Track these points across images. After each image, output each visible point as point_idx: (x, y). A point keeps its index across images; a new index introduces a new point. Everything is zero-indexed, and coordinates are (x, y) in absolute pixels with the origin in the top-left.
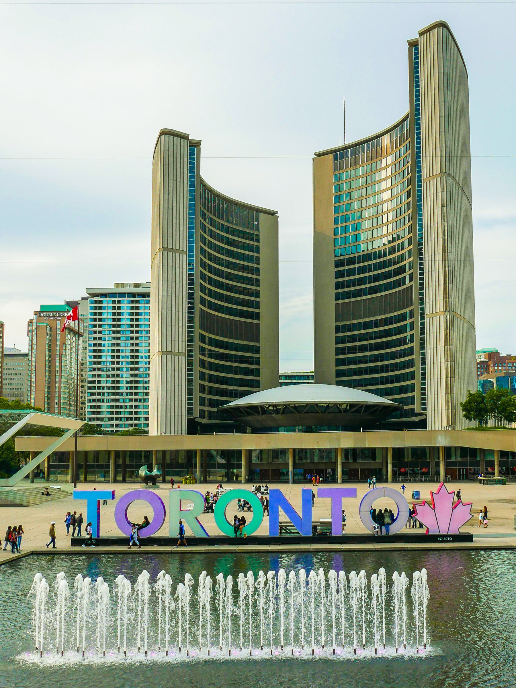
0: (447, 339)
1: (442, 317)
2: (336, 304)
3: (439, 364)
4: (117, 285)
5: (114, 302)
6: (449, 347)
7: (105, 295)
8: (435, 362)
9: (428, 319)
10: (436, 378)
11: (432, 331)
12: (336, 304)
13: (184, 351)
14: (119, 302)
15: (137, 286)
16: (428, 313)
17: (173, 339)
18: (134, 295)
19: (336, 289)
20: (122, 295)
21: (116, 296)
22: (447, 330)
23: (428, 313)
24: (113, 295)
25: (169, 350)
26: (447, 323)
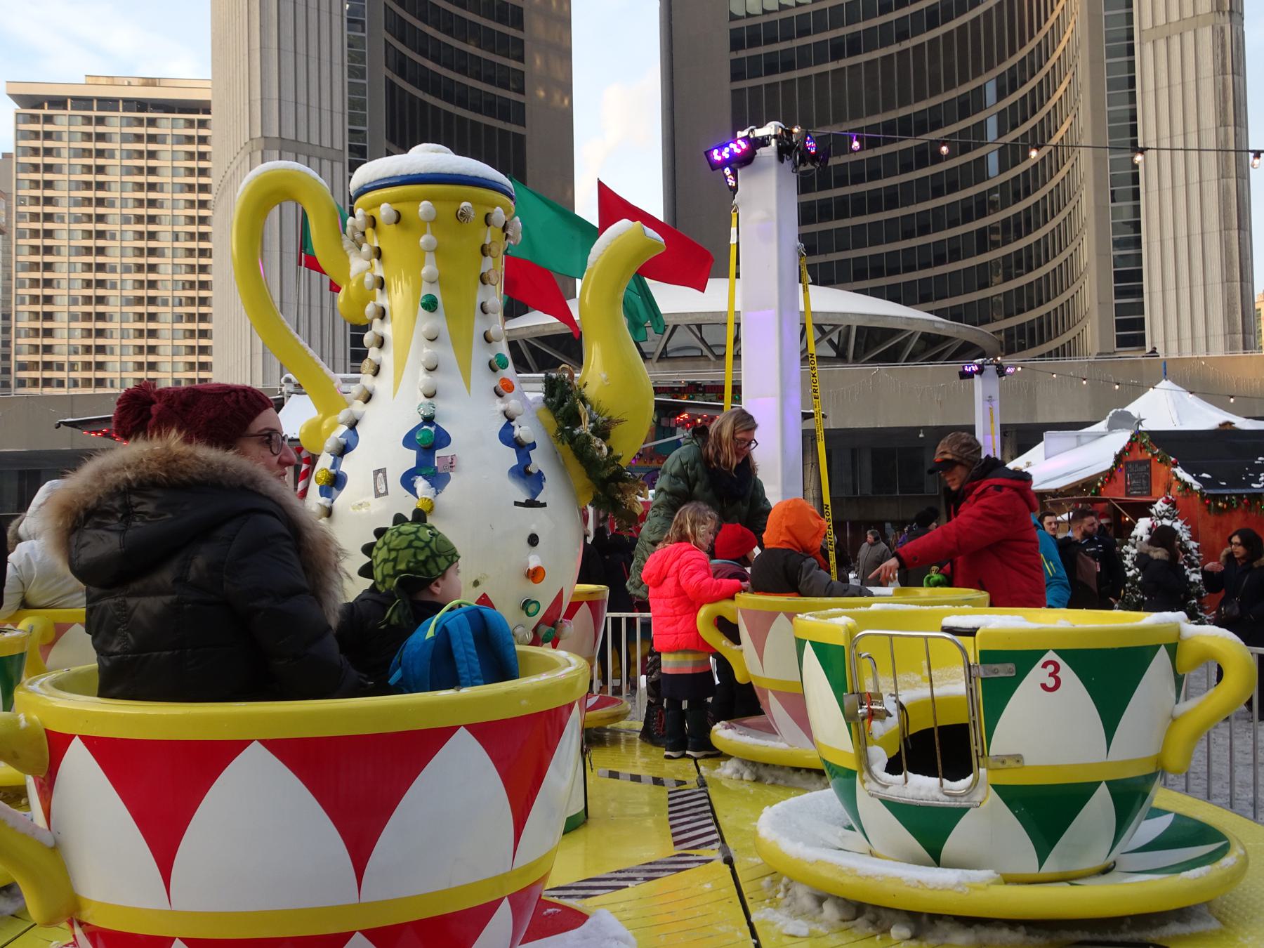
0: (1225, 101)
1: (1206, 35)
2: (733, 91)
3: (1195, 189)
4: (93, 79)
5: (88, 120)
6: (1231, 130)
7: (58, 102)
8: (1180, 181)
9: (1149, 48)
10: (1182, 232)
11: (1163, 82)
12: (733, 91)
13: (338, 146)
14: (101, 121)
15: (150, 82)
16: (1147, 24)
17: (302, 99)
18: (142, 105)
19: (732, 49)
20: (108, 103)
21: (92, 106)
22: (1224, 73)
23: (1147, 24)
24: (82, 102)
25: (289, 134)
26: (1223, 51)
